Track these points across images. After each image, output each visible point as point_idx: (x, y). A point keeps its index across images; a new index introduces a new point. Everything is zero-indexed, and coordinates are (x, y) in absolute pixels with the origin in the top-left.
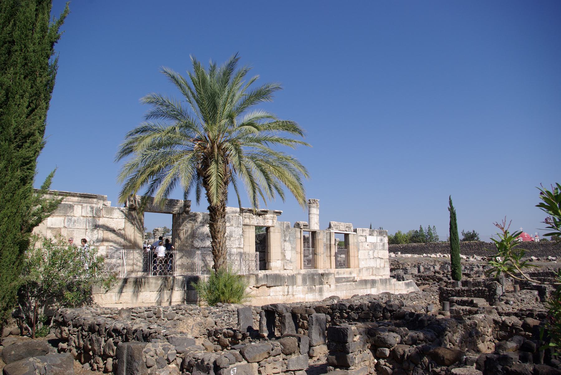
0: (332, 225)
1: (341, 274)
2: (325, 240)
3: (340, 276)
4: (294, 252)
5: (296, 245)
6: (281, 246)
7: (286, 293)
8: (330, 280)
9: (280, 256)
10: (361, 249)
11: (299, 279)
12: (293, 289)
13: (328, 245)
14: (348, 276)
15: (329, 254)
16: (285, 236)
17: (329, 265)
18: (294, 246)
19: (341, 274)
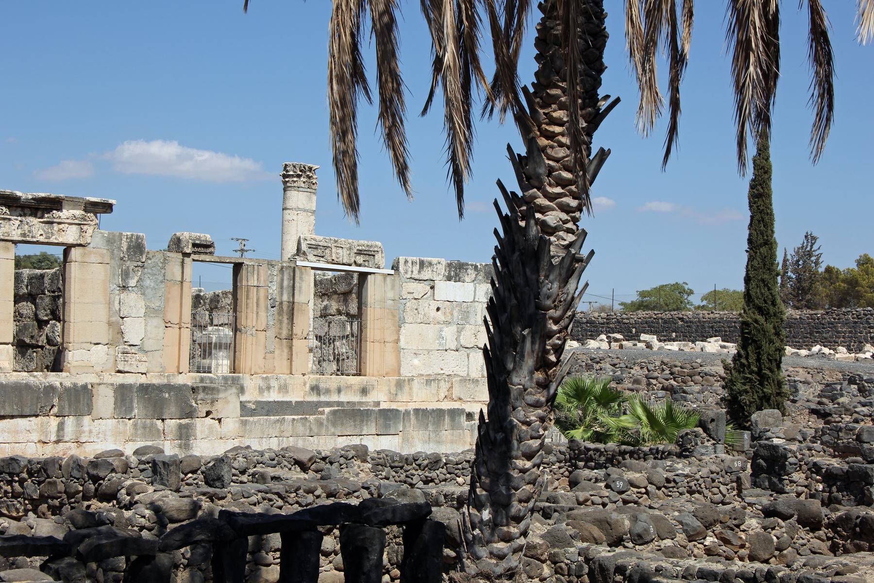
0: (304, 247)
1: (328, 391)
2: (274, 289)
3: (323, 398)
4: (156, 322)
5: (167, 301)
6: (110, 303)
7: (53, 438)
8: (219, 405)
9: (103, 333)
10: (409, 319)
11: (104, 400)
12: (79, 425)
13: (285, 308)
14: (356, 398)
15: (285, 333)
16: (126, 275)
17: (286, 363)
18: (156, 304)
19: (328, 391)
